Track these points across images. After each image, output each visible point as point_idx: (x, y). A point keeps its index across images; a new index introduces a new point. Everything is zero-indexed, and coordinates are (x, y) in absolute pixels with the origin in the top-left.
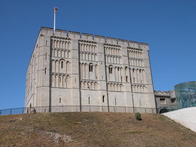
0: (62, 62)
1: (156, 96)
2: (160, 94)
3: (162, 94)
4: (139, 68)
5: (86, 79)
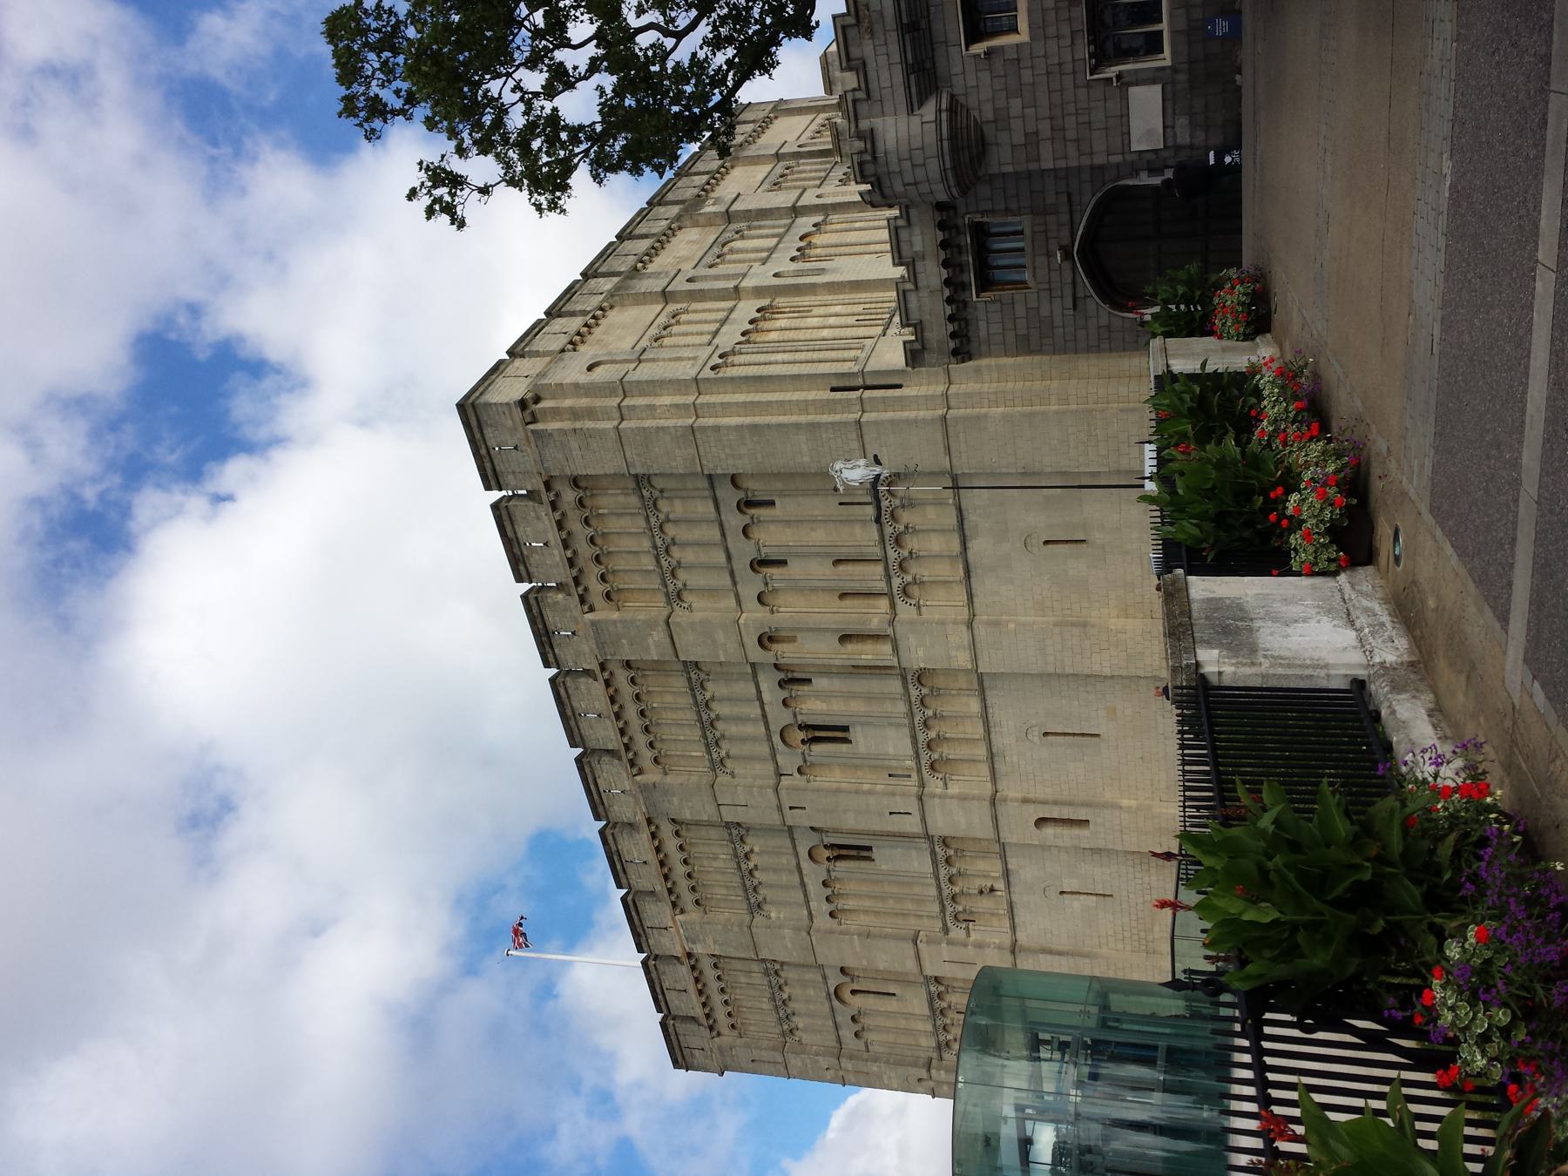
0: (854, 992)
1: (963, 349)
2: (931, 306)
3: (932, 273)
4: (734, 521)
5: (933, 892)
